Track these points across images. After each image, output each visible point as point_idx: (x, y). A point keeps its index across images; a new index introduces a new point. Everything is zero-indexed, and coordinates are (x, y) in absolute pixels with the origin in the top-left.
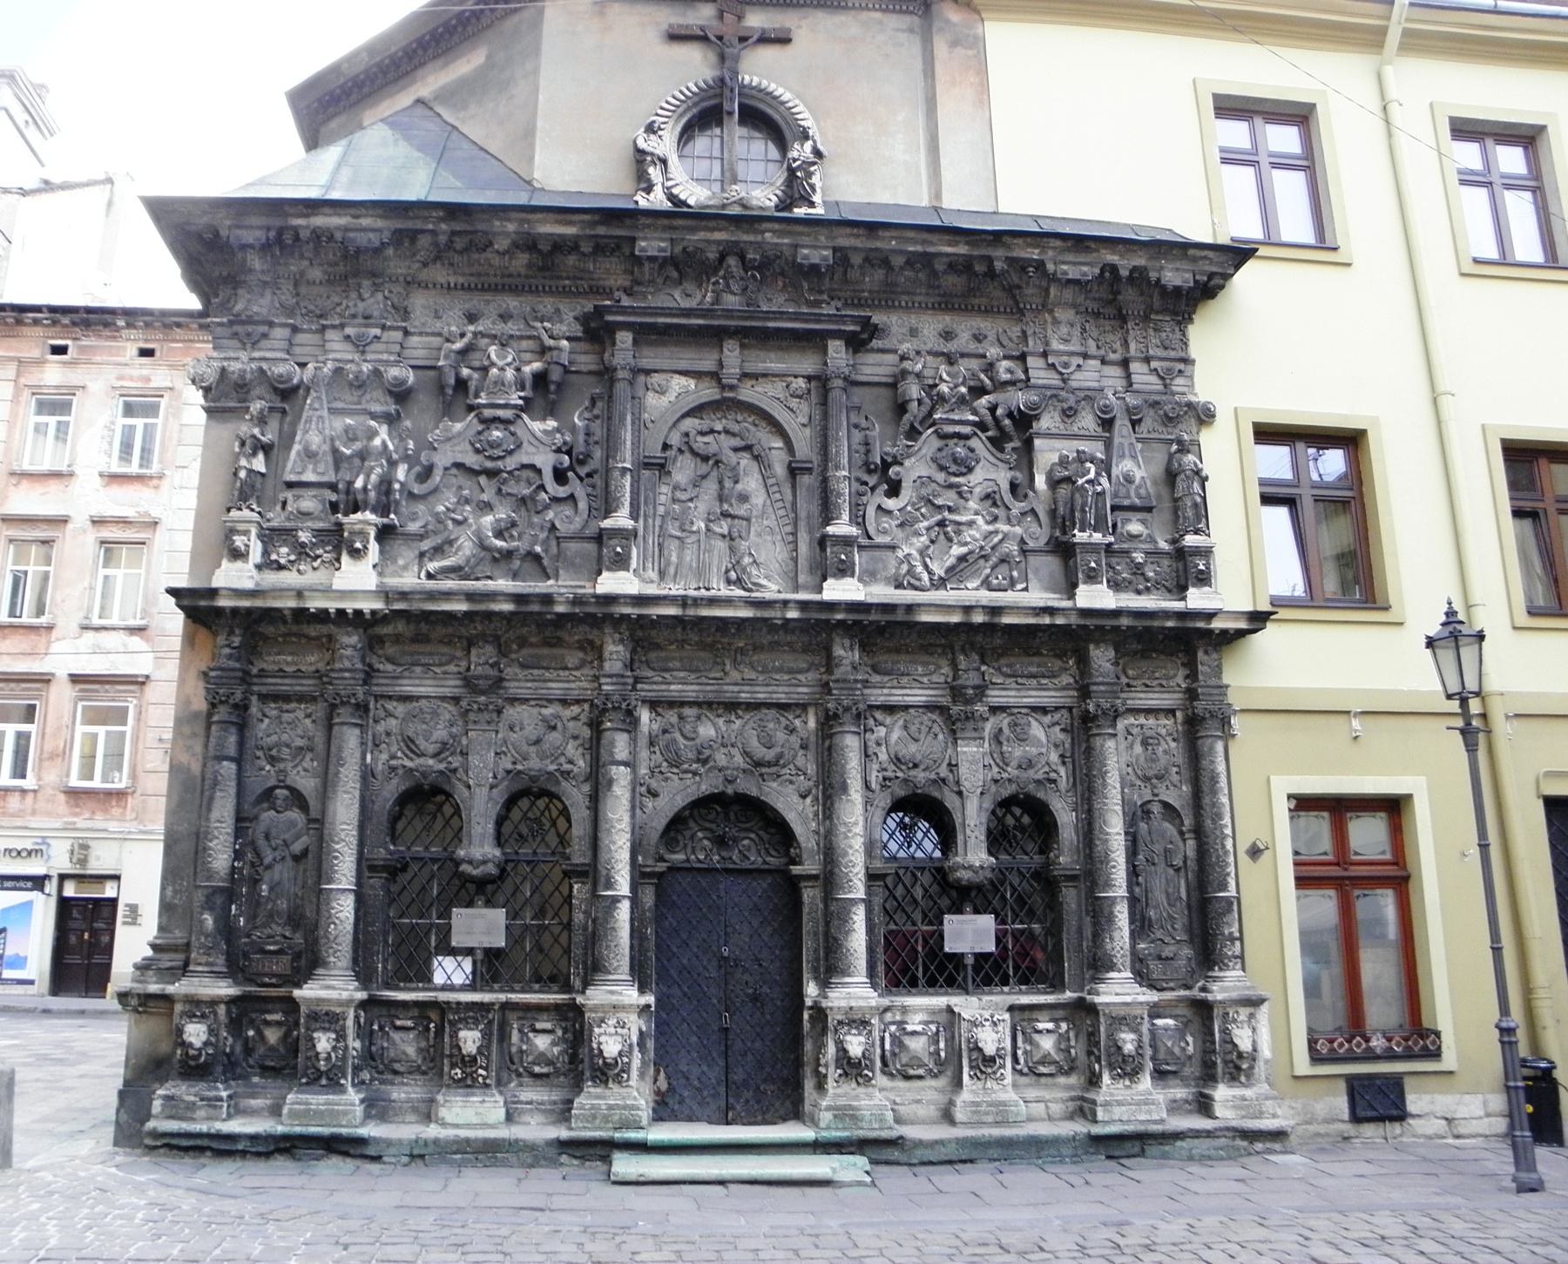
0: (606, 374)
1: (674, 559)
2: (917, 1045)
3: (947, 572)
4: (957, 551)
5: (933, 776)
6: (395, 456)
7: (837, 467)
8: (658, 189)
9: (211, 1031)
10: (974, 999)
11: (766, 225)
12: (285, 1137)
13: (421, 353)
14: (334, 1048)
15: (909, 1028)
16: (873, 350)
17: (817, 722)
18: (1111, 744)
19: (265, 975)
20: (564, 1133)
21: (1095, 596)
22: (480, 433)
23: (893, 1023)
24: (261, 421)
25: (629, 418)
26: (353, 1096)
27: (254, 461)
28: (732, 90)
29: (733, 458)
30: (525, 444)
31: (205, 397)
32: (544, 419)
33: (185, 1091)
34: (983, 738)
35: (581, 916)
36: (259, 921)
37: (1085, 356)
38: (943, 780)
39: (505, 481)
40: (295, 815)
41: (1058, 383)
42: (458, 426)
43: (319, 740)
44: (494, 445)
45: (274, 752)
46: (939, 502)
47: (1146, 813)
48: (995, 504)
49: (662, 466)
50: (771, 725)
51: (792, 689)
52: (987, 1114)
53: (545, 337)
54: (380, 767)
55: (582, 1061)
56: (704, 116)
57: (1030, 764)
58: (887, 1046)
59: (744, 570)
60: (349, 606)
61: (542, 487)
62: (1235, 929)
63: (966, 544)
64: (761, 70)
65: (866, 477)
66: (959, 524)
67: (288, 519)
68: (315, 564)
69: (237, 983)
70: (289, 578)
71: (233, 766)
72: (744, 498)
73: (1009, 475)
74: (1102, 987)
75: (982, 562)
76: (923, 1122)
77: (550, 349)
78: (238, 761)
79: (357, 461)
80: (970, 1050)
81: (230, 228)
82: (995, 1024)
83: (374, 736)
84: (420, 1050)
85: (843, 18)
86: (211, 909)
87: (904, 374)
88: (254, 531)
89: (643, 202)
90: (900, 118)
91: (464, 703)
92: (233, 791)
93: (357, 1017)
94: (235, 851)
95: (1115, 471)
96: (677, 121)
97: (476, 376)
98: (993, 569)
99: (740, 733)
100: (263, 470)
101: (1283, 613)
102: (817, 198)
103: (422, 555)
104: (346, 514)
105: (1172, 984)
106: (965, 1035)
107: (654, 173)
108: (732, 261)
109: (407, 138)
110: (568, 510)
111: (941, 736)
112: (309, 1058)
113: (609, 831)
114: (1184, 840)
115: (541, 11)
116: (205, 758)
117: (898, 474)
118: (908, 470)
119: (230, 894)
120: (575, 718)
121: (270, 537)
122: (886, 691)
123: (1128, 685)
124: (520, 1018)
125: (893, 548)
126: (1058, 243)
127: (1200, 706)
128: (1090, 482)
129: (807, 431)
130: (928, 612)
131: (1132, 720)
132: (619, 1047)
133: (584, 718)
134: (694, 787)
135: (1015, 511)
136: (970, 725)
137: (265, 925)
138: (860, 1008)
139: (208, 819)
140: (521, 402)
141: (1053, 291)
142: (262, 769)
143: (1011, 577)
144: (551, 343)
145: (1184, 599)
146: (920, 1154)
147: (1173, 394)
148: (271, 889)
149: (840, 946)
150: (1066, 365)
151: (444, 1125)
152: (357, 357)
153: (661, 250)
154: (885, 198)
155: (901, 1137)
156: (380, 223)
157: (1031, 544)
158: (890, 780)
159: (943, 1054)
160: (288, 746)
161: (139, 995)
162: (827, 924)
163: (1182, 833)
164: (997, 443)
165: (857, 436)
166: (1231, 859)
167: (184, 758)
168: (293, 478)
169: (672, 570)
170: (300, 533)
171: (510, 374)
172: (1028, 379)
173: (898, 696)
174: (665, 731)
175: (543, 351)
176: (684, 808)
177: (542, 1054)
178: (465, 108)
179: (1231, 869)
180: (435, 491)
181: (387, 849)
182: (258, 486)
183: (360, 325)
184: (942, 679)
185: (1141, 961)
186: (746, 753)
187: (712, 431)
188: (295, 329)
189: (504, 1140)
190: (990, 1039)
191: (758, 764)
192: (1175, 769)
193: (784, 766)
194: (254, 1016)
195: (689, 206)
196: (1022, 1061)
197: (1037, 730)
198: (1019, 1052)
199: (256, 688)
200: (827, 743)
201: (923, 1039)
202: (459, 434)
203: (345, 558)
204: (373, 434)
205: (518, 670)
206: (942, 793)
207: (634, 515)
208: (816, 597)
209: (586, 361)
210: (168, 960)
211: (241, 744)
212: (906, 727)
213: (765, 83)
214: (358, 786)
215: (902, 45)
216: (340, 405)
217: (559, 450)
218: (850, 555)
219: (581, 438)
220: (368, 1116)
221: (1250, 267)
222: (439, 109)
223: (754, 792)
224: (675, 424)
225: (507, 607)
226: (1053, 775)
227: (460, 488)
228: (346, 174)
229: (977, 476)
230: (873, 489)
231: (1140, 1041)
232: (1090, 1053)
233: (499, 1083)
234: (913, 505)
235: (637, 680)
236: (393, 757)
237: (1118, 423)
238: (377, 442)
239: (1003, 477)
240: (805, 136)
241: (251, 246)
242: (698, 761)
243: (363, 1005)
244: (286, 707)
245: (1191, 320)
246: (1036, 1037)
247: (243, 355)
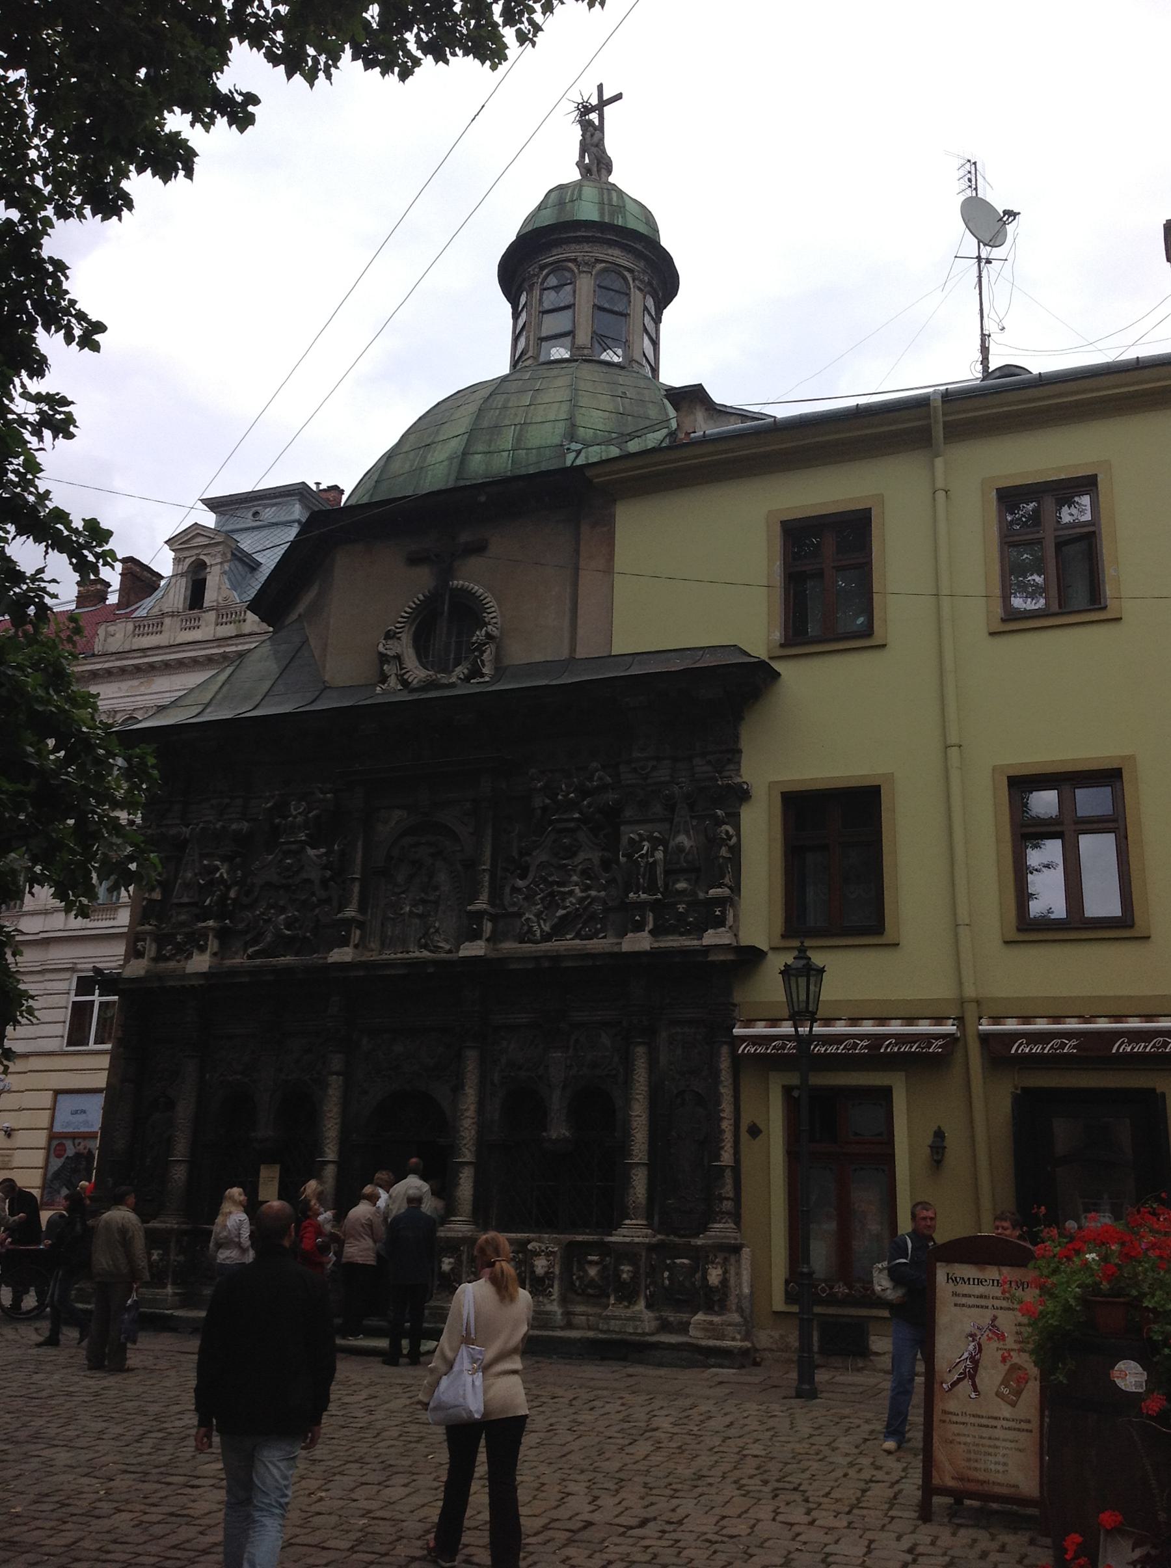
4: (561, 912)
8: (392, 681)
14: (161, 1260)
21: (640, 942)
22: (280, 861)
25: (360, 844)
26: (169, 1290)
60: (186, 983)
61: (313, 894)
62: (728, 1190)
66: (565, 893)
70: (172, 964)
82: (548, 1254)
95: (672, 844)
102: (485, 671)
121: (161, 940)
128: (642, 856)
138: (453, 1238)
154: (538, 658)
166: (728, 1136)
171: (300, 819)
196: (577, 1284)
204: (218, 869)
207: (362, 909)
217: (325, 868)
218: (480, 925)
226: (614, 1072)
229: (582, 856)
238: (218, 875)
239: (596, 857)
245: (742, 718)
246: (587, 1267)
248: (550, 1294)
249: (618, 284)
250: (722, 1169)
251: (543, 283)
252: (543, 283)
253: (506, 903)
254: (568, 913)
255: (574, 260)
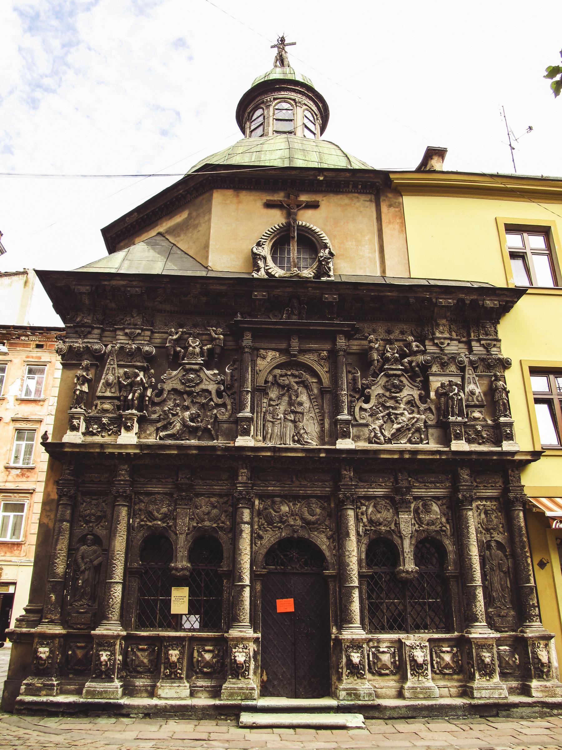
0: (240, 350)
1: (270, 431)
2: (386, 658)
3: (391, 436)
4: (396, 426)
5: (388, 529)
6: (146, 385)
7: (342, 390)
8: (262, 270)
9: (51, 651)
10: (411, 636)
11: (309, 285)
12: (83, 704)
13: (158, 341)
14: (109, 660)
15: (381, 650)
16: (356, 339)
17: (335, 504)
18: (470, 513)
19: (79, 624)
20: (217, 702)
22: (184, 375)
23: (373, 647)
24: (86, 369)
25: (250, 369)
26: (117, 683)
27: (83, 387)
28: (294, 227)
29: (296, 387)
30: (204, 380)
31: (62, 359)
32: (212, 370)
33: (37, 682)
34: (411, 511)
35: (227, 595)
36: (77, 598)
37: (451, 339)
38: (393, 530)
39: (195, 397)
40: (95, 548)
41: (438, 351)
42: (175, 373)
43: (109, 513)
44: (191, 381)
45: (87, 518)
46: (388, 404)
47: (489, 547)
48: (412, 406)
49: (265, 390)
50: (314, 506)
51: (323, 489)
52: (421, 693)
53: (213, 334)
54: (136, 525)
55: (227, 666)
56: (281, 240)
57: (433, 523)
58: (371, 659)
59: (301, 436)
61: (211, 400)
62: (535, 601)
63: (400, 423)
64: (306, 218)
65: (355, 395)
67: (98, 413)
68: (109, 433)
69: (64, 628)
71: (68, 525)
72: (301, 404)
73: (418, 392)
74: (473, 630)
75: (407, 432)
76: (390, 698)
77: (216, 339)
78: (71, 522)
79: (129, 388)
80: (410, 661)
81: (75, 285)
82: (421, 648)
83: (134, 510)
84: (150, 661)
85: (341, 196)
86: (54, 592)
87: (371, 348)
88: (82, 418)
89: (255, 276)
90: (367, 238)
91: (175, 496)
92: (67, 536)
93: (121, 644)
94: (67, 564)
95: (467, 390)
96: (270, 241)
97: (183, 351)
98: (413, 434)
99: (300, 508)
100: (87, 391)
101: (547, 453)
102: (331, 273)
103: (157, 430)
104: (124, 411)
105: (506, 629)
106: (408, 654)
107: (261, 263)
108: (295, 301)
109: (154, 249)
110: (223, 410)
111: (391, 511)
112: (97, 665)
113: (240, 554)
114: (507, 559)
115: (212, 195)
116: (56, 521)
117: (369, 392)
118: (373, 391)
119: (63, 585)
120: (225, 503)
121: (89, 421)
122: (365, 490)
123: (477, 486)
124: (197, 645)
125: (367, 425)
126: (438, 290)
127: (511, 495)
129: (328, 375)
130: (384, 454)
131: (479, 503)
132: (244, 658)
133: (230, 503)
134: (279, 535)
135: (422, 408)
136: (404, 505)
137: (80, 600)
138: (357, 639)
139: (55, 549)
140: (202, 362)
141: (436, 310)
142: (82, 526)
143: (421, 438)
144: (216, 336)
145: (501, 446)
146: (388, 713)
147: (492, 355)
148: (82, 583)
149: (348, 609)
150: (442, 343)
151: (160, 698)
152: (130, 342)
153: (264, 296)
155: (379, 705)
156: (141, 284)
157: (430, 423)
158: (368, 530)
159: (397, 663)
160: (94, 515)
161: (17, 633)
162: (341, 599)
163: (506, 556)
164: (412, 379)
165: (350, 376)
167: (46, 521)
168: (100, 394)
169: (269, 436)
170: (103, 419)
171: (198, 350)
172: (426, 350)
173: (372, 492)
174: (266, 509)
175: (212, 340)
176: (274, 544)
177: (208, 662)
178: (179, 236)
179: (531, 572)
180: (165, 401)
181: (138, 563)
182: (85, 398)
183: (131, 329)
184: (391, 484)
185: (491, 618)
186: (303, 519)
187: (286, 375)
188: (103, 330)
189: (188, 705)
190: (420, 656)
191: (308, 523)
192: (501, 525)
193: (320, 524)
194: (72, 644)
195: (276, 277)
196: (436, 667)
197: (435, 508)
198: (434, 662)
199: (80, 489)
200: (339, 514)
201: (388, 655)
202: (175, 376)
203: (123, 430)
205: (200, 481)
206: (393, 536)
207: (252, 411)
208: (333, 447)
209: (231, 344)
210: (33, 617)
211: (73, 514)
212: (375, 506)
213: (308, 225)
214: (126, 533)
215: (367, 207)
216: (122, 363)
217: (219, 383)
219: (229, 378)
220: (124, 694)
221: (524, 298)
222: (168, 237)
223: (307, 536)
224: (270, 372)
225: (194, 452)
227: (175, 400)
228: (127, 263)
230: (358, 399)
231: (493, 657)
232: (468, 663)
233: (188, 678)
234: (376, 406)
235: (254, 485)
236: (142, 521)
237: (467, 368)
238: (139, 379)
239: (416, 393)
240: (325, 246)
241: (84, 293)
242: (281, 522)
243: (124, 638)
244: (94, 497)
245: (499, 323)
246: (442, 655)
247: (80, 341)
248: (427, 675)
249: (312, 119)
250: (531, 588)
251: (275, 106)
252: (275, 106)
253: (357, 417)
254: (403, 427)
255: (294, 100)
